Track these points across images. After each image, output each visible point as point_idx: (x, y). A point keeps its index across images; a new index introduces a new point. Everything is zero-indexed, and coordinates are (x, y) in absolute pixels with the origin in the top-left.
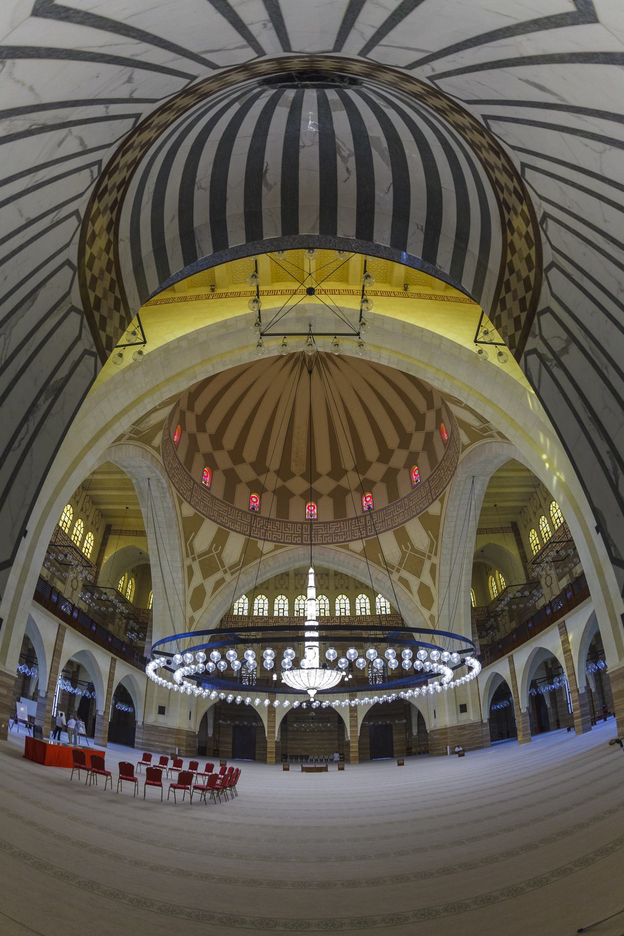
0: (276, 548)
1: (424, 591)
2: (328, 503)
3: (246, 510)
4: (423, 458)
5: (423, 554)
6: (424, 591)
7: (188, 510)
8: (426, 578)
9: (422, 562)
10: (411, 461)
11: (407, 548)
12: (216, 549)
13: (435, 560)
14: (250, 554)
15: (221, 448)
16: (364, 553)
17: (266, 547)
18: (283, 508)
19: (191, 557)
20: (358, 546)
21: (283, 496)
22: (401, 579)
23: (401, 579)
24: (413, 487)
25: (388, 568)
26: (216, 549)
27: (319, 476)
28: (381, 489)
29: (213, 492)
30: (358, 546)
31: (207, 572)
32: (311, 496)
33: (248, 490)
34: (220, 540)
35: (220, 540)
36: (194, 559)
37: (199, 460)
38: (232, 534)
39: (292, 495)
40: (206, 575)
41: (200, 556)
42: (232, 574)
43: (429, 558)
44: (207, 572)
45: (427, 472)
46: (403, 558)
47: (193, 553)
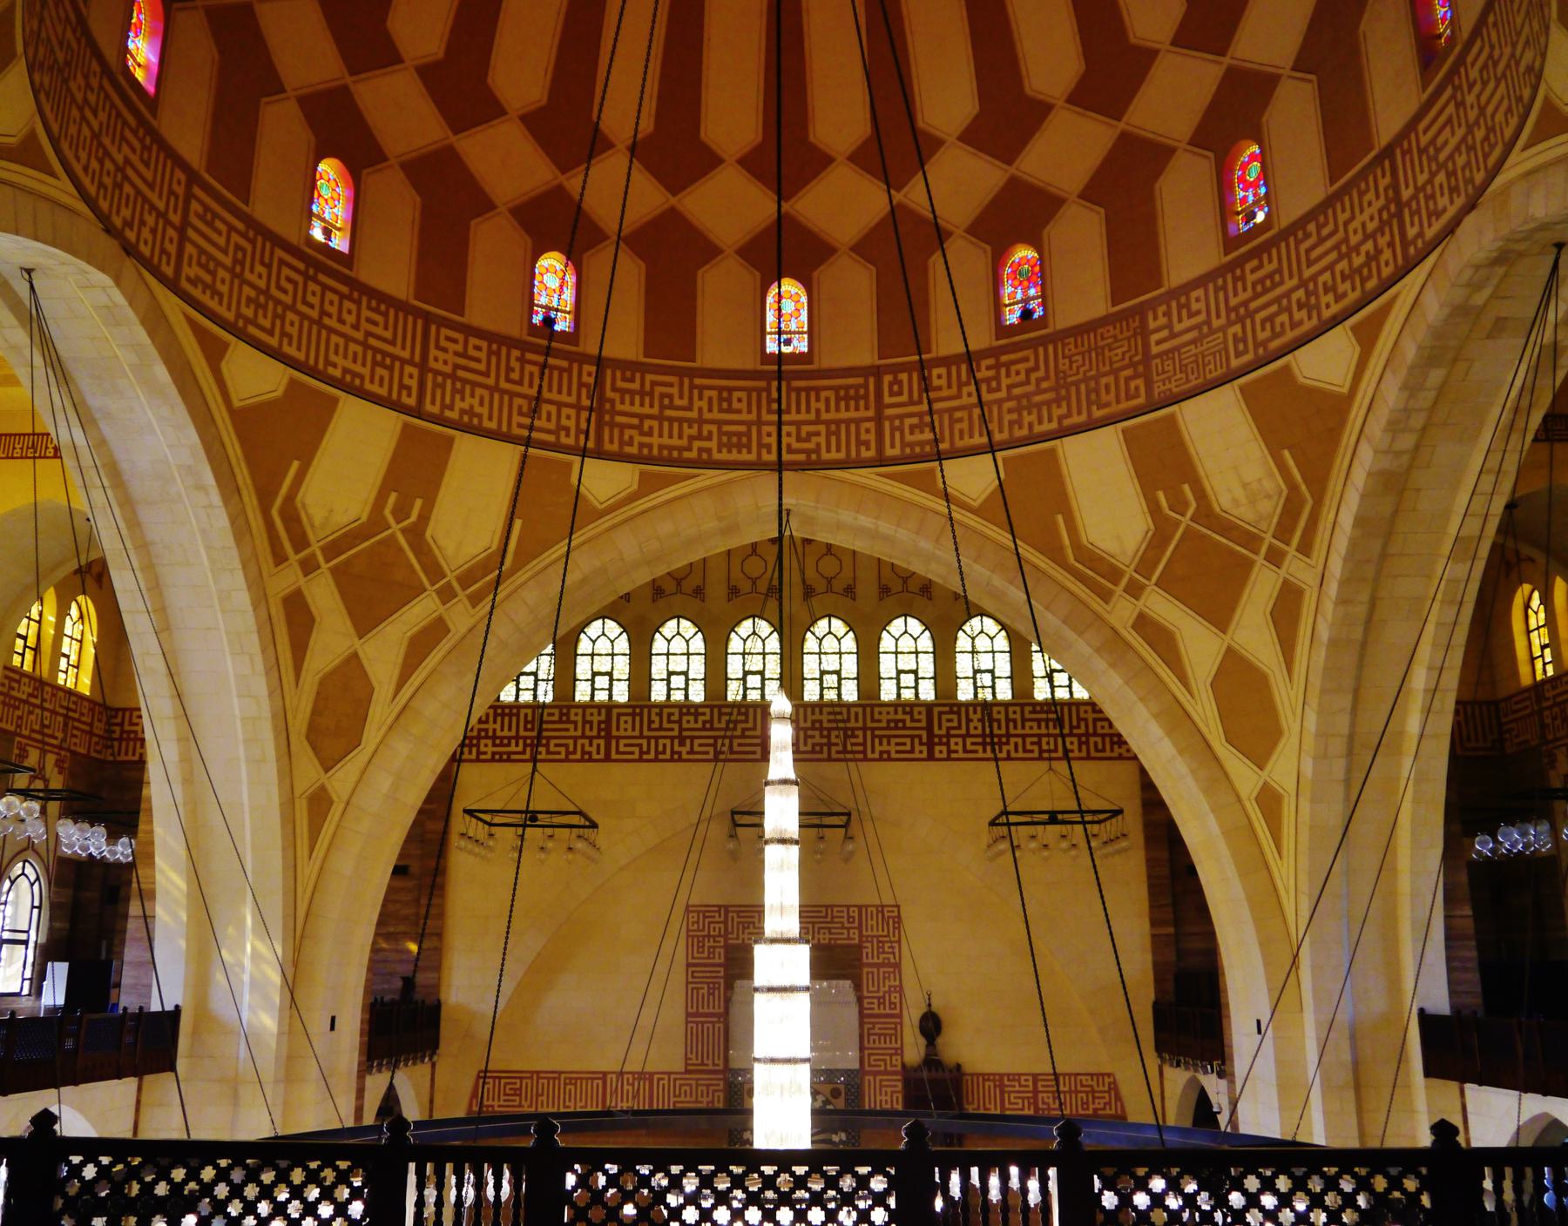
0: (648, 485)
1: (1240, 686)
2: (855, 281)
3: (516, 331)
4: (1295, 110)
5: (1251, 541)
6: (1240, 686)
7: (255, 377)
10: (1236, 111)
11: (1179, 505)
12: (401, 512)
13: (1297, 568)
14: (544, 513)
15: (388, 56)
17: (603, 481)
18: (672, 319)
19: (294, 558)
20: (973, 478)
21: (673, 254)
23: (1143, 623)
24: (1230, 242)
25: (1099, 572)
26: (401, 512)
27: (822, 161)
28: (1081, 232)
29: (367, 273)
31: (370, 599)
32: (785, 251)
33: (519, 240)
34: (414, 474)
35: (414, 474)
36: (308, 567)
37: (281, 125)
38: (465, 445)
39: (709, 251)
40: (365, 619)
41: (332, 550)
42: (475, 600)
43: (1275, 558)
44: (370, 599)
45: (1307, 184)
47: (300, 542)
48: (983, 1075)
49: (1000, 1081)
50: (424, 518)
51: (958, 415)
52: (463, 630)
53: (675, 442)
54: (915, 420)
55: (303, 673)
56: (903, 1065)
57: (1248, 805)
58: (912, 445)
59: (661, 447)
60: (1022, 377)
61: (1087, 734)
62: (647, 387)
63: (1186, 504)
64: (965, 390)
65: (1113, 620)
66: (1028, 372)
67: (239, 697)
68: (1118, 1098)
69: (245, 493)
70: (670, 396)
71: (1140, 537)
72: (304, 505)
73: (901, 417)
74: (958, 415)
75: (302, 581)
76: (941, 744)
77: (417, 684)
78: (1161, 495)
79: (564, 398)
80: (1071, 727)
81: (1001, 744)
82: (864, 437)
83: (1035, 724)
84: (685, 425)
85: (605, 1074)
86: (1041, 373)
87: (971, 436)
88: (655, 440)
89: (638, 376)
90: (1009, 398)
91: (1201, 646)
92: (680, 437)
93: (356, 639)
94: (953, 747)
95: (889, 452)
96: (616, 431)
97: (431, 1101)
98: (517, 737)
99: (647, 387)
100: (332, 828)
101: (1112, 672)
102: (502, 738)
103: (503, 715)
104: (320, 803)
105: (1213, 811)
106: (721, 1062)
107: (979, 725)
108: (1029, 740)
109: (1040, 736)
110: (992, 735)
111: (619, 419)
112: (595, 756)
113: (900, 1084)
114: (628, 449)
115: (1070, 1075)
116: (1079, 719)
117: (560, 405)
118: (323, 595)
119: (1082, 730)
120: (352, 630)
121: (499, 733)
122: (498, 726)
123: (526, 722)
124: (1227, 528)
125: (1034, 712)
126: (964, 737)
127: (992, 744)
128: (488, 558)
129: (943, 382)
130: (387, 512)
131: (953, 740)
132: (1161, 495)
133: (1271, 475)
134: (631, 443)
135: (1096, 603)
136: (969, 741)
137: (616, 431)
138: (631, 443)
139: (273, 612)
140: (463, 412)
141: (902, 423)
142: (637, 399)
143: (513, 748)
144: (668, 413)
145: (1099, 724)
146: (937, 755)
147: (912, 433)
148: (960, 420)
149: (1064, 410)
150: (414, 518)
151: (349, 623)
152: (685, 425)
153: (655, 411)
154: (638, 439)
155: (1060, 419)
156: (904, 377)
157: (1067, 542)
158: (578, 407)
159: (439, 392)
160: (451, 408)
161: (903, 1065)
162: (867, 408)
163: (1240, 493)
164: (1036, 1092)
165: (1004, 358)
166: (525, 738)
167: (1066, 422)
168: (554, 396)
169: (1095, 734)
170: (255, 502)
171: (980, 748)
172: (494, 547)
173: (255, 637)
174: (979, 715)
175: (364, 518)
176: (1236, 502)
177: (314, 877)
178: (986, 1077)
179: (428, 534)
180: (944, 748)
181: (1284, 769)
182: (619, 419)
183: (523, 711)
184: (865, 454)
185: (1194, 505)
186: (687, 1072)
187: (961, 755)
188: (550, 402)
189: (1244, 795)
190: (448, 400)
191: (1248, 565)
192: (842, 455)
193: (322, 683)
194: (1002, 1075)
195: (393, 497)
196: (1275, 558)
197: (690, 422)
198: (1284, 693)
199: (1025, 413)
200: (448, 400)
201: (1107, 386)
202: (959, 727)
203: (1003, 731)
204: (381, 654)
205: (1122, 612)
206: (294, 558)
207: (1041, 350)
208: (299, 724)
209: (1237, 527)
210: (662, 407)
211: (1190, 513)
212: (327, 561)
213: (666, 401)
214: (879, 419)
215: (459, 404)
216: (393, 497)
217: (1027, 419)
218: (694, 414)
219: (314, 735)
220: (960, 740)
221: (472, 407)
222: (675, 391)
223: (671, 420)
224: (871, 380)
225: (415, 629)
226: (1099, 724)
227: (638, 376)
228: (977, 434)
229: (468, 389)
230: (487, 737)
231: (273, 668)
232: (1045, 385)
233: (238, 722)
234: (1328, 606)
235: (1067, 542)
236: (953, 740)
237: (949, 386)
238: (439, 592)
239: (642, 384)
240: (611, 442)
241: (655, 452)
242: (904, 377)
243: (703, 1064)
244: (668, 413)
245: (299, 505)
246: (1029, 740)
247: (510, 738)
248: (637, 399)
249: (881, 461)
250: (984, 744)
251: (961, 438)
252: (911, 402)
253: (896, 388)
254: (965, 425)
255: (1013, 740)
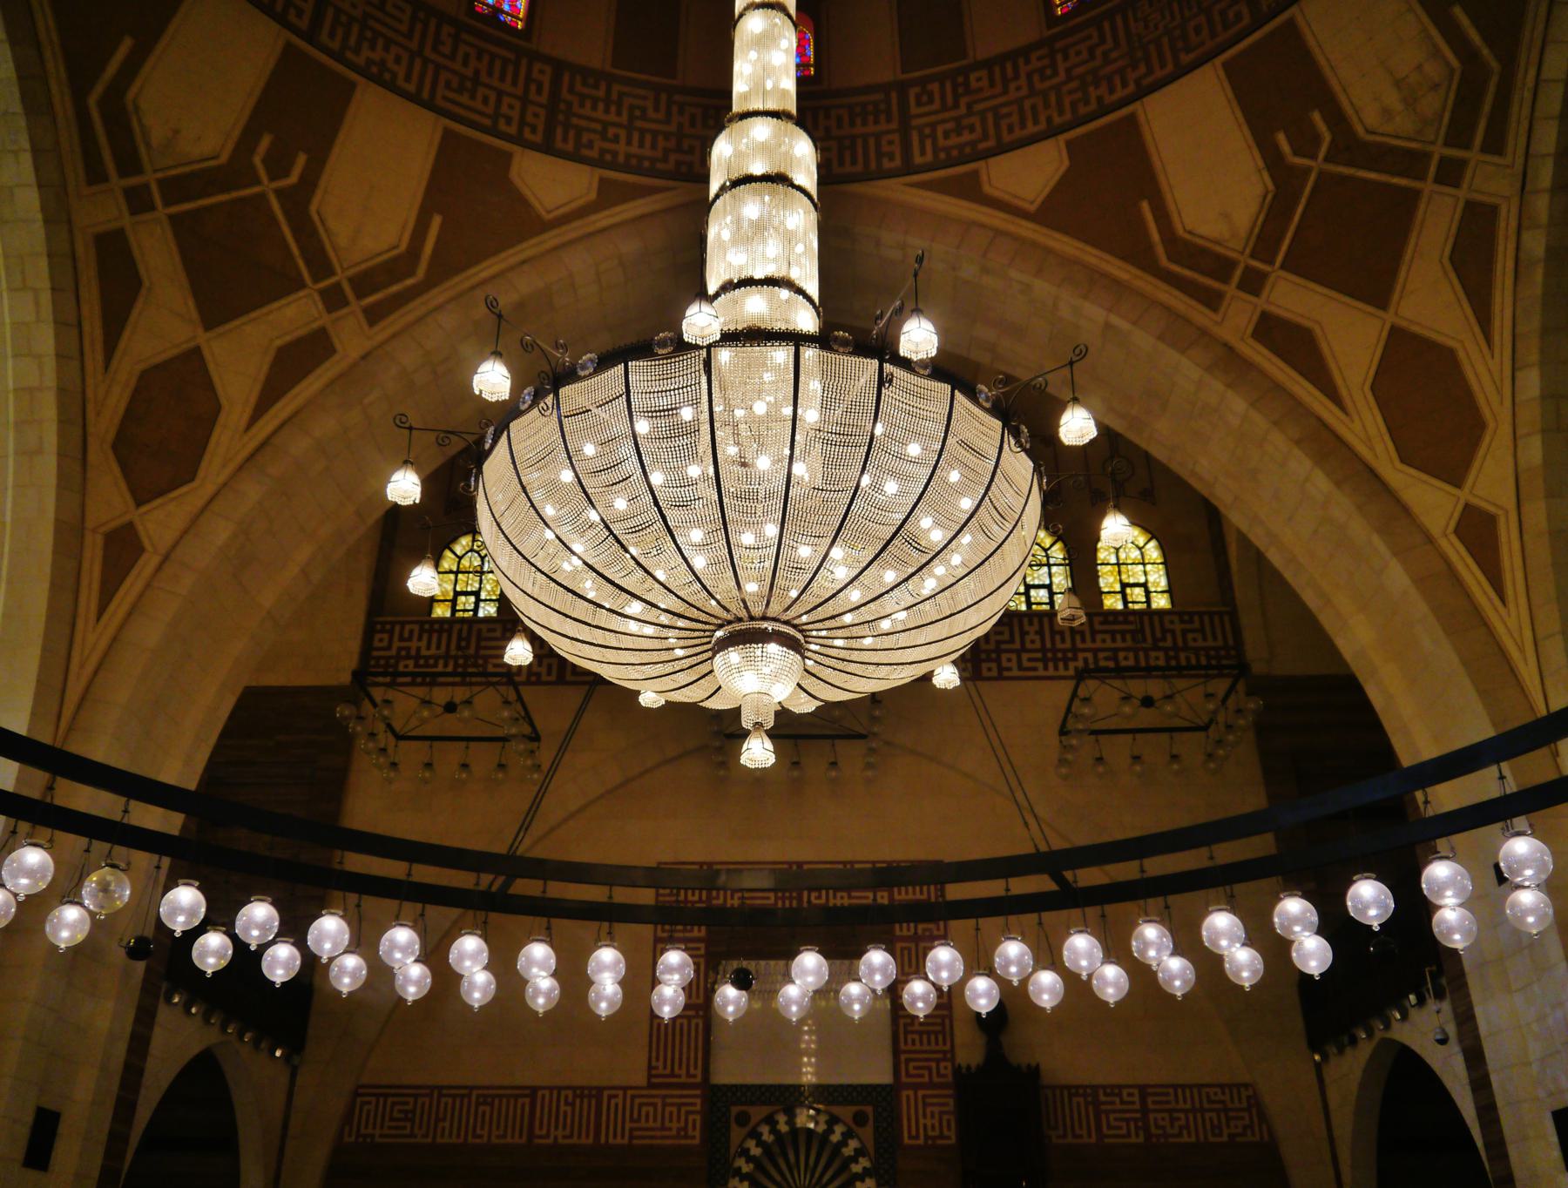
0: (608, 195)
8: (1429, 299)
9: (1400, 212)
12: (277, 166)
13: (1489, 179)
16: (1056, 211)
17: (548, 182)
20: (1031, 173)
22: (1270, 330)
23: (1270, 330)
25: (1203, 270)
30: (1031, 173)
31: (224, 291)
34: (300, 114)
36: (138, 202)
41: (176, 188)
43: (1451, 174)
46: (1277, 210)
47: (129, 163)
48: (1069, 1087)
49: (1092, 1094)
50: (310, 182)
51: (1005, 110)
52: (354, 354)
53: (647, 152)
54: (948, 126)
55: (118, 354)
56: (957, 1070)
57: (1444, 543)
58: (947, 150)
59: (628, 156)
60: (1085, 55)
61: (1175, 647)
62: (614, 96)
63: (1316, 139)
64: (1012, 86)
65: (1227, 333)
66: (1091, 51)
67: (15, 356)
68: (1263, 1117)
69: (48, 54)
70: (644, 110)
71: (1254, 208)
72: (137, 108)
73: (933, 126)
74: (1005, 110)
75: (127, 221)
76: (989, 660)
77: (284, 415)
78: (1281, 138)
79: (507, 87)
80: (1155, 640)
81: (1066, 661)
82: (885, 148)
83: (1108, 637)
84: (660, 138)
85: (533, 1091)
86: (1110, 43)
87: (1023, 126)
88: (622, 147)
89: (603, 86)
90: (1070, 79)
91: (1351, 337)
92: (654, 147)
93: (200, 331)
94: (1005, 664)
95: (918, 160)
96: (572, 134)
97: (285, 1127)
98: (447, 657)
99: (614, 96)
100: (139, 585)
101: (1230, 393)
102: (427, 658)
103: (431, 632)
104: (123, 547)
105: (1395, 554)
106: (699, 1072)
107: (1037, 638)
108: (1101, 655)
109: (1116, 650)
110: (1054, 650)
111: (575, 121)
112: (544, 678)
113: (951, 1101)
114: (585, 152)
115: (1191, 1087)
116: (1164, 631)
117: (500, 94)
118: (156, 251)
119: (1169, 643)
120: (195, 314)
121: (424, 652)
122: (423, 644)
123: (460, 638)
124: (1378, 155)
125: (1105, 622)
126: (1019, 652)
127: (1055, 660)
128: (395, 259)
129: (985, 83)
130: (257, 160)
131: (1004, 657)
132: (1281, 138)
133: (1436, 53)
134: (590, 145)
135: (1200, 315)
136: (1025, 656)
137: (572, 134)
138: (590, 145)
139: (80, 249)
140: (370, 62)
141: (934, 130)
142: (601, 106)
143: (440, 669)
144: (639, 124)
145: (1190, 636)
146: (985, 673)
147: (946, 135)
148: (1009, 115)
149: (1143, 69)
150: (293, 178)
151: (191, 304)
152: (660, 138)
153: (624, 118)
154: (598, 144)
155: (1138, 82)
156: (935, 87)
157: (1155, 236)
158: (525, 101)
159: (340, 32)
160: (357, 51)
161: (957, 1070)
162: (889, 120)
163: (1393, 99)
164: (1145, 1111)
165: (1058, 45)
166: (456, 658)
167: (1146, 82)
168: (496, 83)
169: (1186, 648)
170: (63, 74)
171: (1040, 665)
172: (403, 247)
173: (43, 263)
174: (1036, 627)
175: (224, 158)
176: (1387, 113)
177: (103, 644)
178: (1073, 1090)
179: (313, 208)
180: (994, 665)
181: (1491, 480)
182: (575, 121)
183: (456, 627)
184: (887, 164)
185: (1327, 138)
186: (651, 1086)
187: (1015, 673)
188: (487, 86)
189: (1435, 531)
190: (353, 40)
191: (1410, 199)
192: (859, 168)
193: (145, 376)
194: (1095, 1088)
195: (265, 142)
196: (1451, 174)
197: (667, 136)
198: (1481, 369)
199: (1091, 89)
200: (353, 40)
201: (1198, 31)
202: (1012, 641)
203: (1068, 645)
204: (238, 358)
205: (1235, 320)
206: (117, 183)
207: (1107, 26)
208: (105, 425)
209: (1392, 150)
210: (631, 118)
211: (1321, 155)
212: (167, 204)
213: (638, 113)
214: (905, 129)
215: (366, 53)
216: (265, 142)
217: (1093, 93)
218: (673, 128)
219: (123, 446)
220: (1014, 657)
221: (383, 63)
222: (650, 104)
223: (642, 131)
224: (894, 95)
225: (288, 338)
226: (1190, 636)
227: (603, 86)
228: (1030, 123)
229: (380, 43)
230: (408, 657)
231: (68, 324)
232: (1114, 55)
233: (11, 396)
234: (1541, 206)
235: (1155, 236)
236: (1004, 657)
237: (992, 84)
238: (323, 293)
239: (609, 90)
240: (565, 140)
241: (621, 159)
242: (935, 87)
243: (672, 1075)
244: (639, 124)
245: (130, 107)
246: (1101, 655)
247: (437, 658)
248: (601, 106)
249: (908, 169)
250: (1045, 661)
251: (1011, 129)
252: (944, 108)
253: (925, 98)
254: (1015, 118)
255: (1081, 656)
